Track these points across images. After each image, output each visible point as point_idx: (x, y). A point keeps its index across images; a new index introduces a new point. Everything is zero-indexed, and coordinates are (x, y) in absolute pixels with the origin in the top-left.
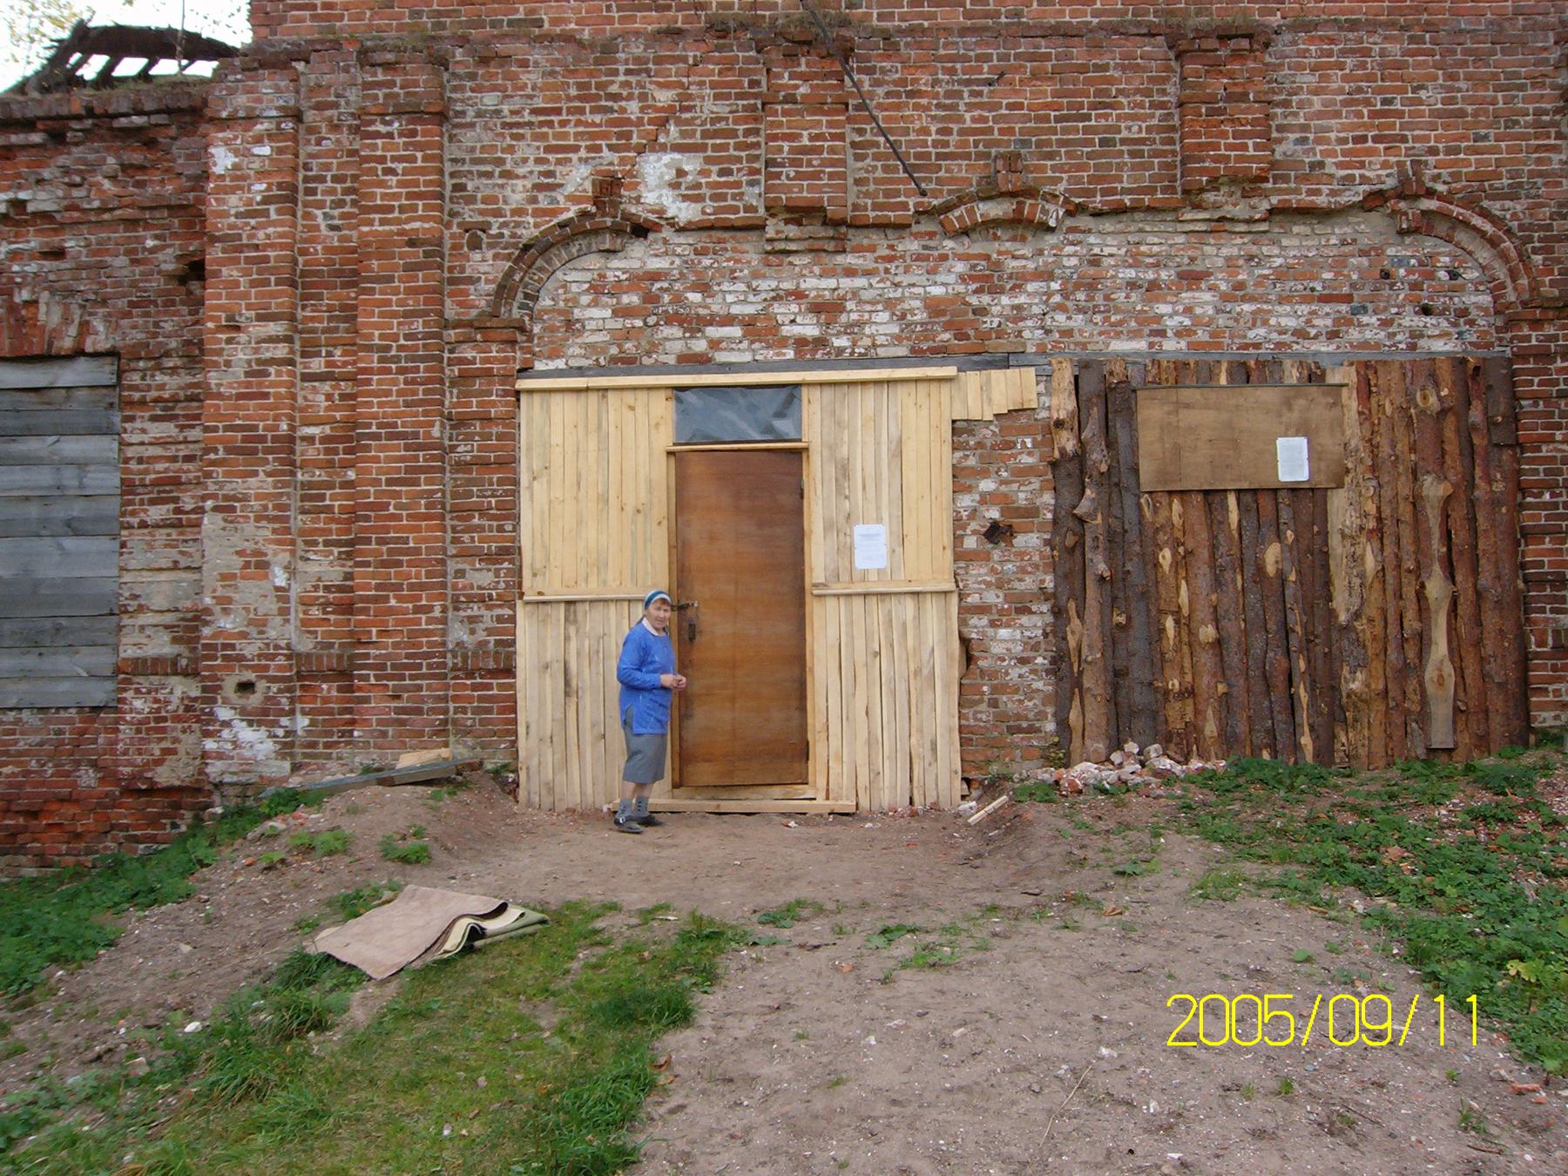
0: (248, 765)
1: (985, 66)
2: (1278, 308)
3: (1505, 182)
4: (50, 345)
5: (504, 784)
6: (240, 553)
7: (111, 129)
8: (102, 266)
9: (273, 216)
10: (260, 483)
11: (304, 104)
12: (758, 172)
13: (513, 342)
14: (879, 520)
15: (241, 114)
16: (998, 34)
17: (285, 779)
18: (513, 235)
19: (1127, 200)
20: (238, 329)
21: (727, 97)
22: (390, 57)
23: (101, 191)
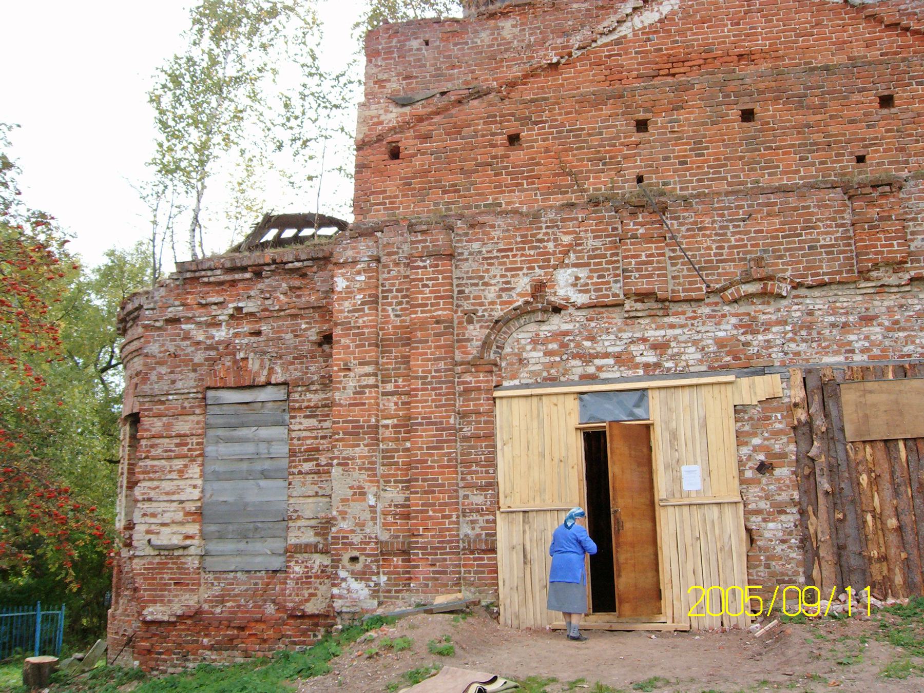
0: (355, 602)
1: (741, 211)
2: (920, 334)
4: (254, 380)
5: (492, 613)
6: (351, 488)
8: (280, 339)
9: (367, 311)
10: (361, 450)
11: (381, 254)
12: (618, 275)
13: (491, 372)
14: (696, 463)
15: (350, 260)
16: (746, 194)
17: (375, 610)
18: (490, 315)
19: (826, 279)
20: (349, 370)
21: (600, 237)
22: (424, 227)
23: (279, 301)
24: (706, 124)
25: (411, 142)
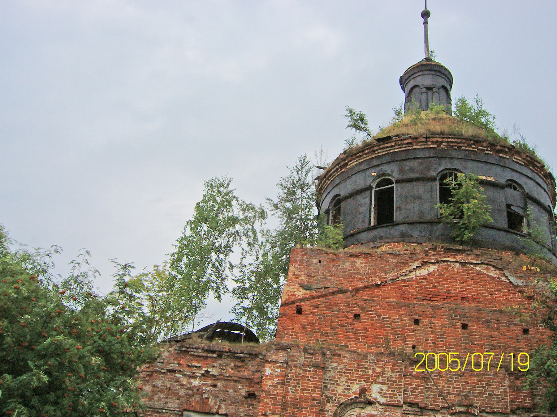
4: (210, 410)
7: (234, 356)
9: (279, 388)
18: (338, 400)
21: (394, 372)
22: (312, 352)
24: (445, 327)
25: (308, 308)
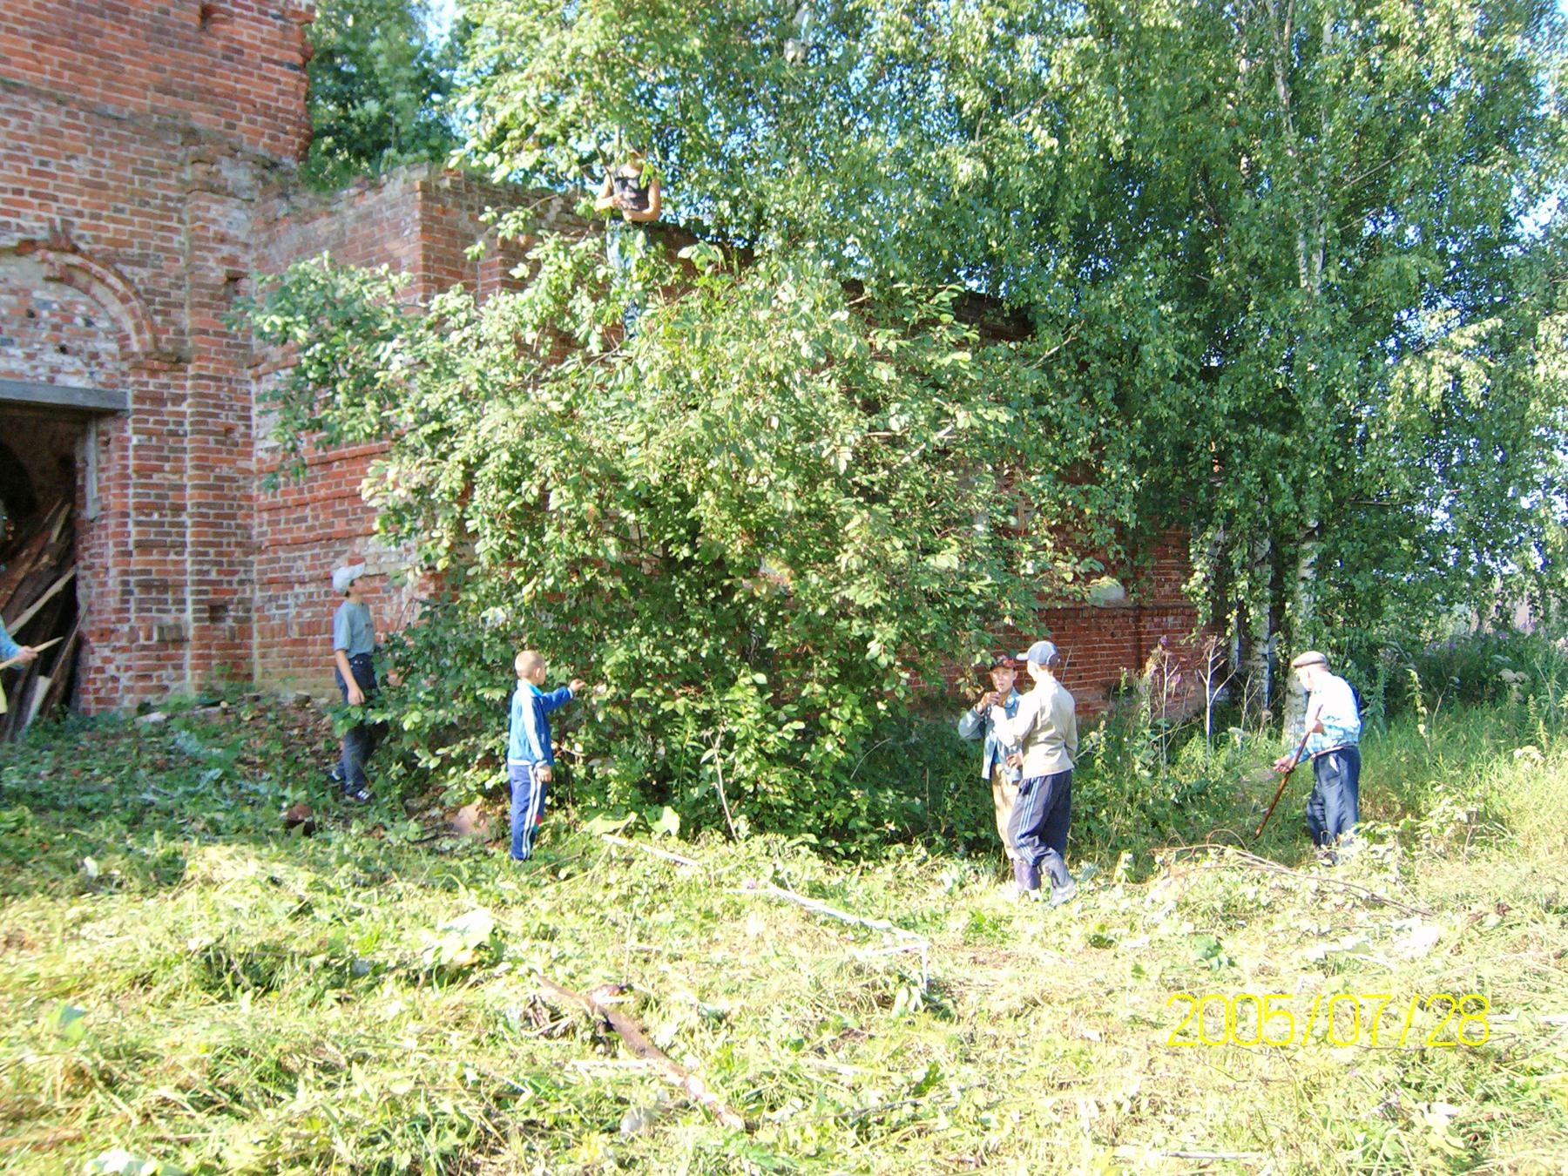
3: (136, 251)
